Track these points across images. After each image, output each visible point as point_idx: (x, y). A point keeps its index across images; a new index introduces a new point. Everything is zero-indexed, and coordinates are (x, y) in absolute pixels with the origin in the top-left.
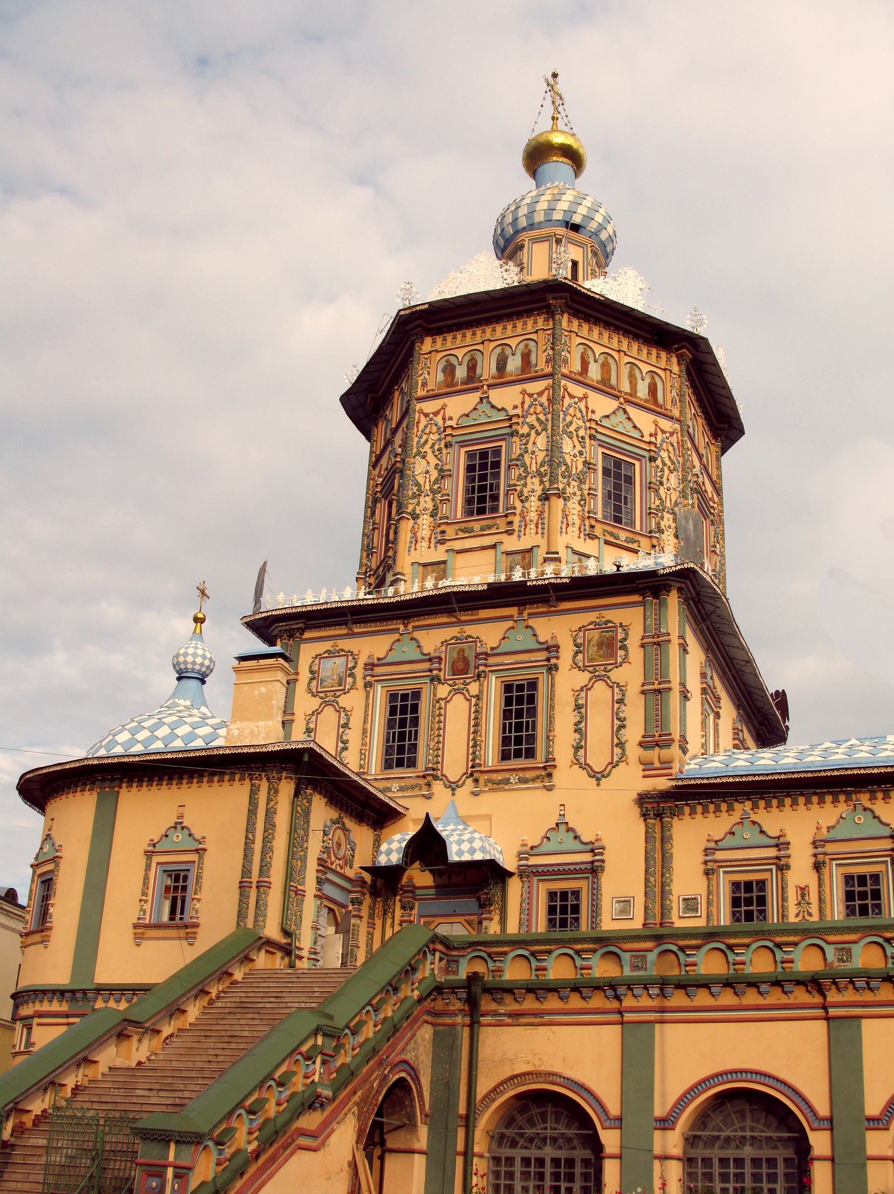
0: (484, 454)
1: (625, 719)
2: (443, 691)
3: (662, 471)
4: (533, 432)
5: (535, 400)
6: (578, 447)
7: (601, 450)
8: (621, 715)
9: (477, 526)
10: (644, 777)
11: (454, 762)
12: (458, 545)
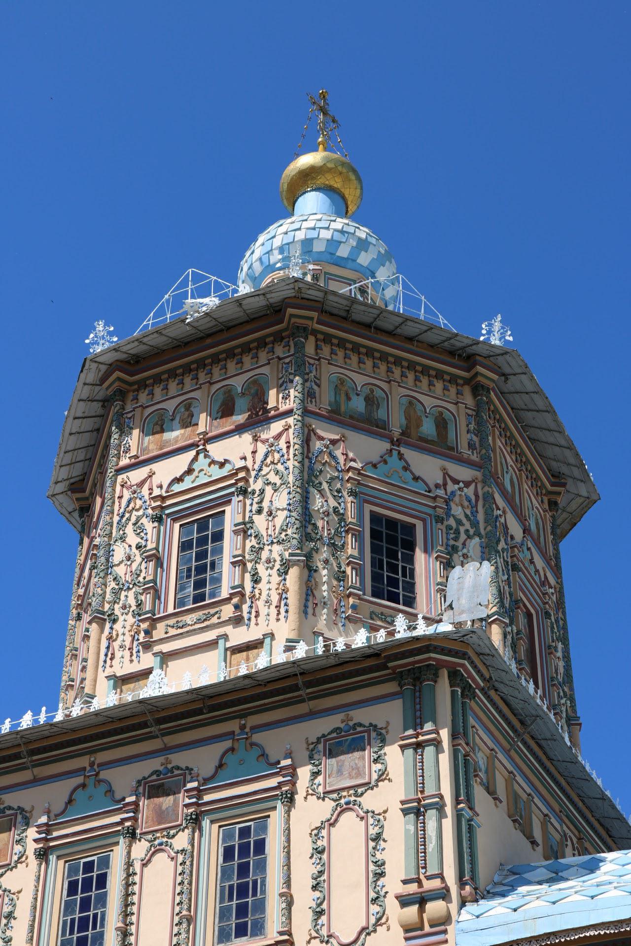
0: (203, 525)
1: (383, 864)
2: (140, 849)
3: (457, 532)
4: (269, 490)
5: (272, 445)
6: (332, 503)
7: (368, 508)
9: (189, 619)
10: (407, 939)
12: (166, 648)
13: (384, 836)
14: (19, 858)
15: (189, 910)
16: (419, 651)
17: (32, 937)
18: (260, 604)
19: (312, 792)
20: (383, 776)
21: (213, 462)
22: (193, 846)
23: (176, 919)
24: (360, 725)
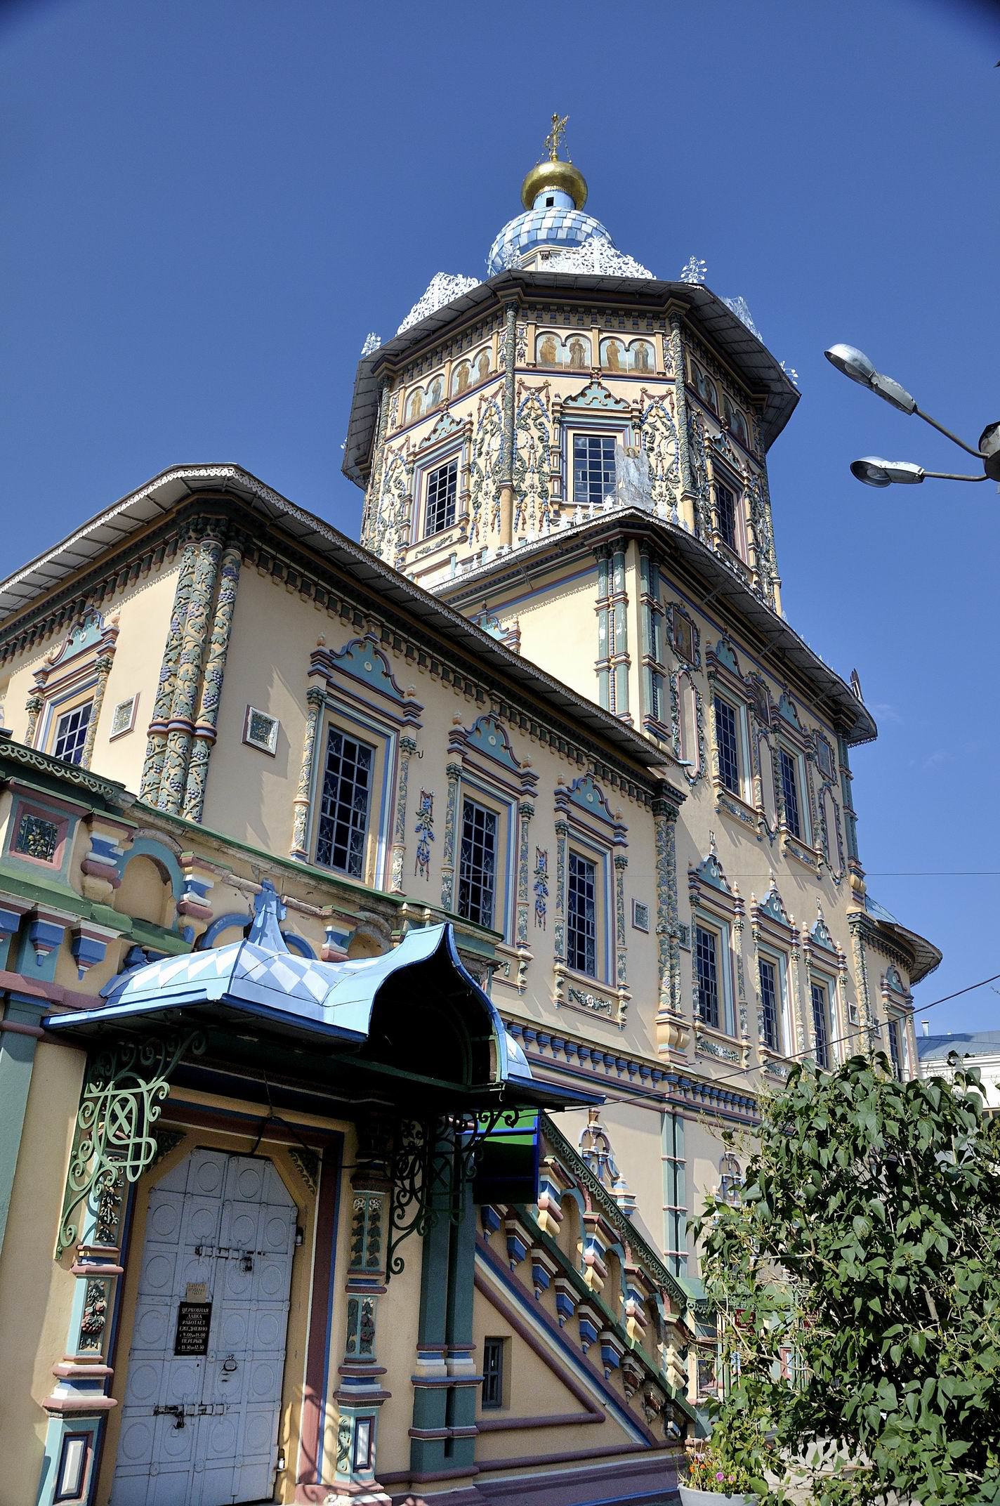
0: (443, 472)
9: (432, 544)
18: (480, 525)
21: (453, 421)
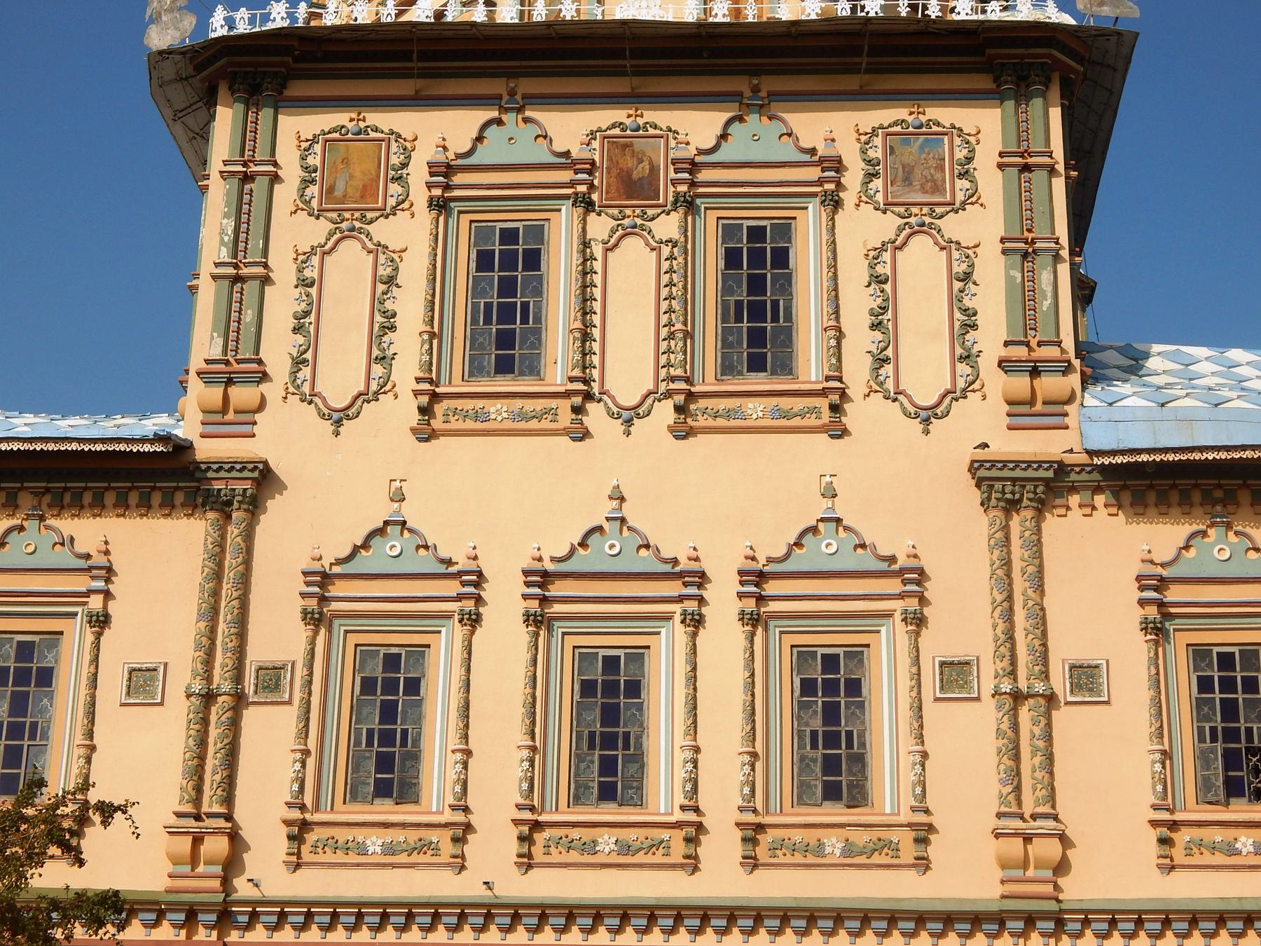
2: (599, 226)
8: (967, 303)
11: (630, 364)
13: (975, 277)
14: (399, 204)
15: (686, 325)
16: (1038, 42)
17: (433, 317)
19: (866, 196)
20: (973, 197)
22: (686, 236)
23: (664, 332)
24: (938, 124)
